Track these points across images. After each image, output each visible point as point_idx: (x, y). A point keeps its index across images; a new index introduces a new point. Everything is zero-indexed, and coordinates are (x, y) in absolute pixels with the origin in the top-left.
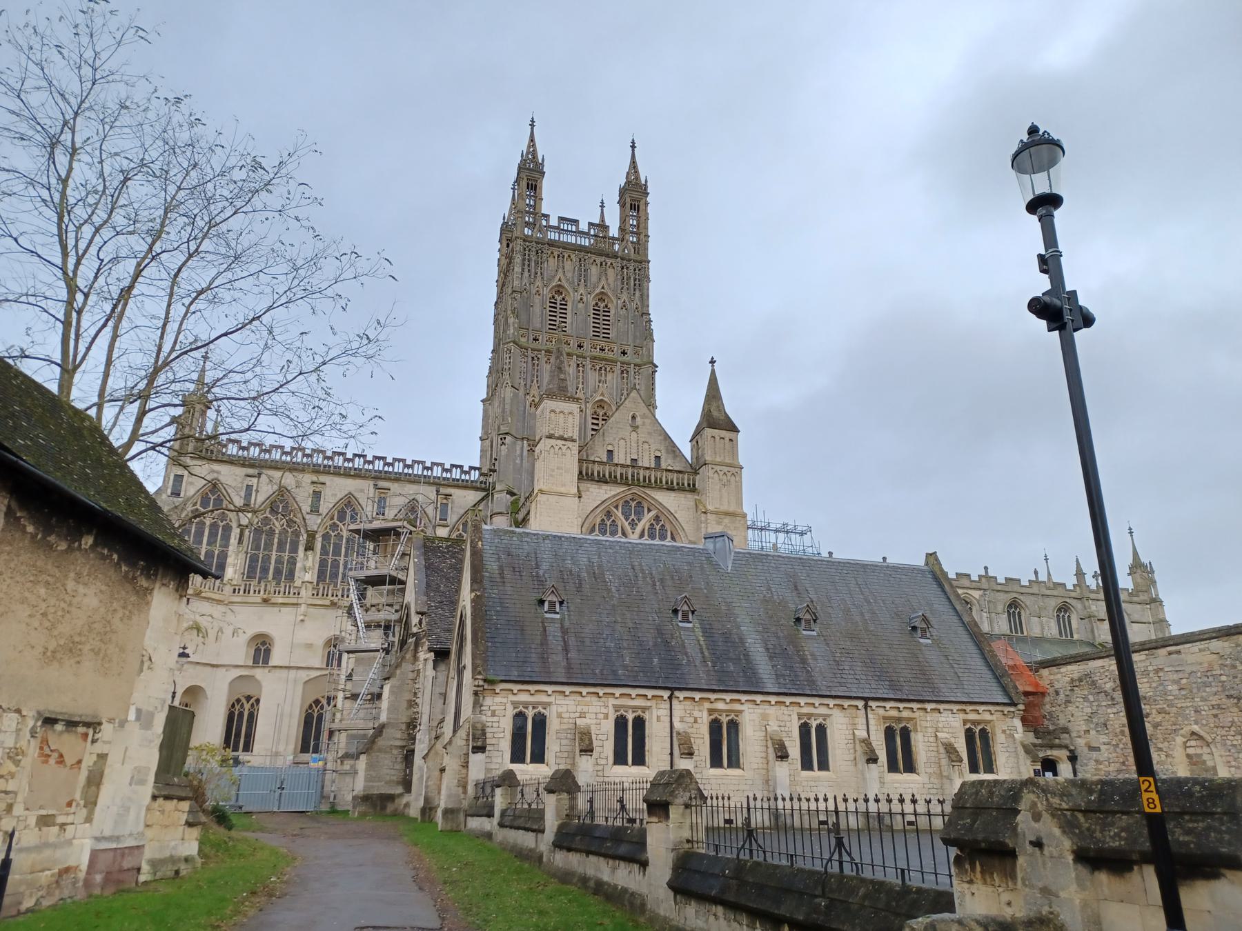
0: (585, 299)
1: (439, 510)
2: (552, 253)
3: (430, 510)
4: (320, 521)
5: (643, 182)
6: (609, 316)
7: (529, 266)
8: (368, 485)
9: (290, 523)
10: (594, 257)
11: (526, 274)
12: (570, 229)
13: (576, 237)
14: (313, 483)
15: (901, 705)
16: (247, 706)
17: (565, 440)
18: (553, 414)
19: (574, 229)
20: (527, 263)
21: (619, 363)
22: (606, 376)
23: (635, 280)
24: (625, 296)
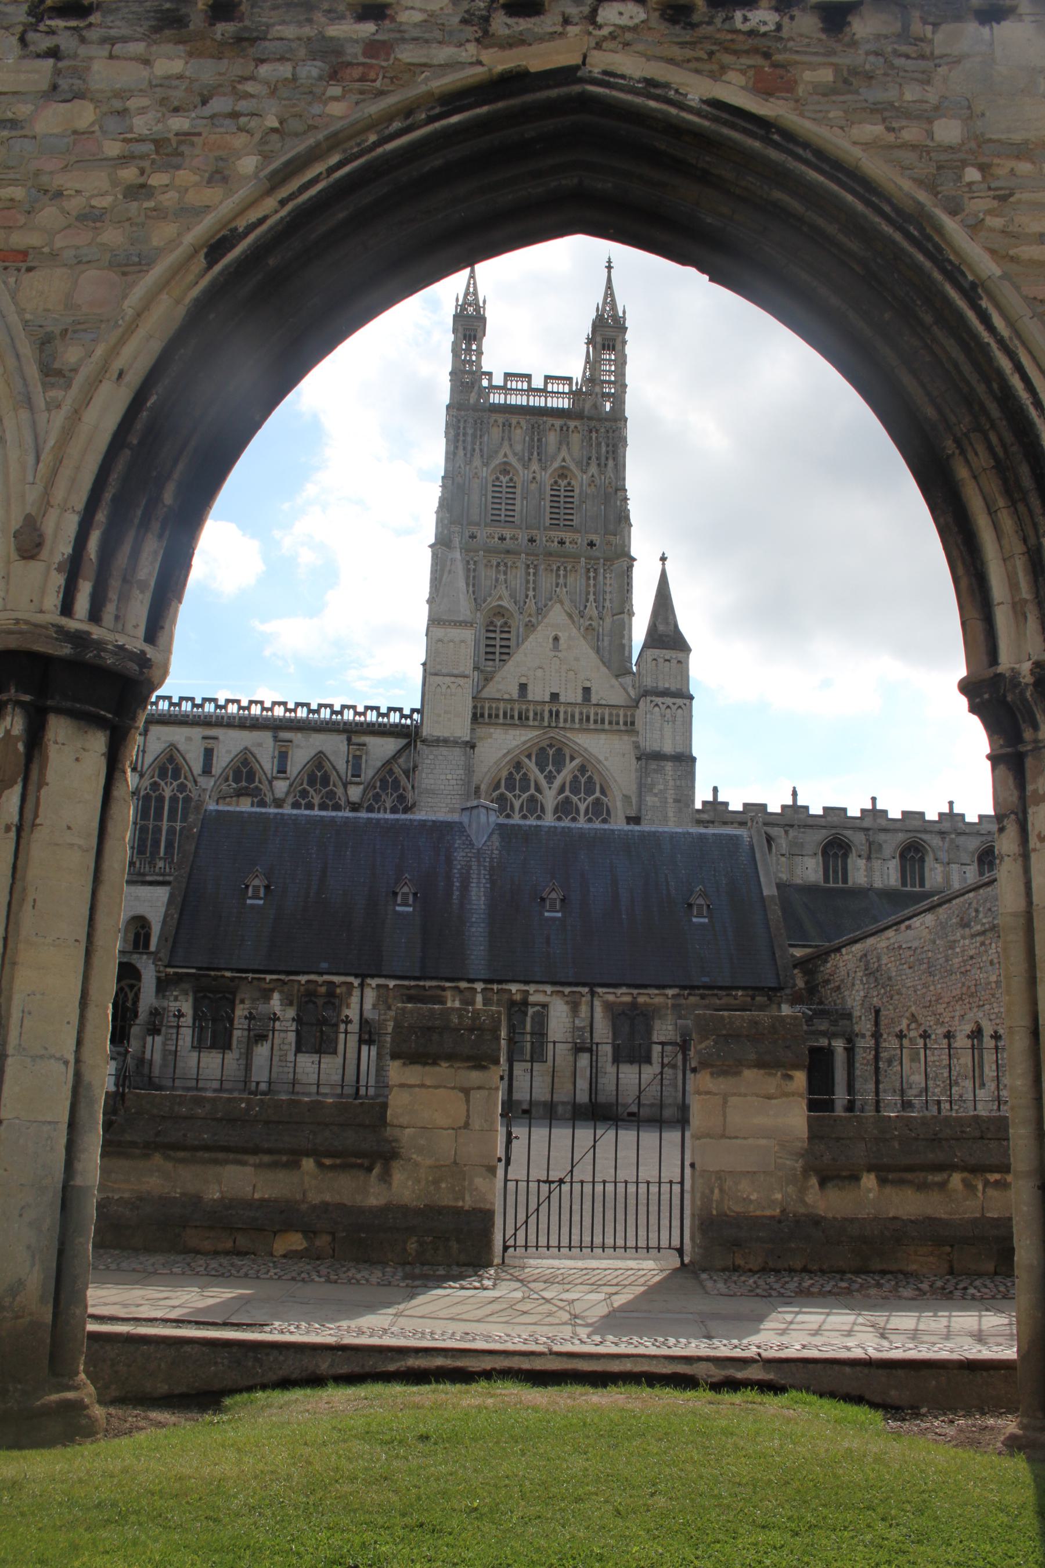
0: (538, 477)
1: (350, 764)
2: (496, 421)
3: (341, 766)
4: (212, 783)
5: (621, 314)
6: (573, 497)
7: (464, 441)
8: (267, 737)
9: (182, 788)
10: (550, 421)
11: (461, 453)
12: (520, 387)
13: (528, 396)
14: (205, 738)
15: (635, 992)
16: (131, 996)
17: (456, 676)
18: (440, 644)
19: (525, 387)
20: (461, 438)
21: (583, 559)
22: (565, 576)
23: (608, 446)
24: (593, 469)
